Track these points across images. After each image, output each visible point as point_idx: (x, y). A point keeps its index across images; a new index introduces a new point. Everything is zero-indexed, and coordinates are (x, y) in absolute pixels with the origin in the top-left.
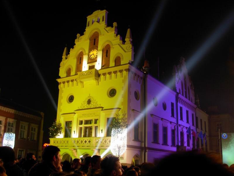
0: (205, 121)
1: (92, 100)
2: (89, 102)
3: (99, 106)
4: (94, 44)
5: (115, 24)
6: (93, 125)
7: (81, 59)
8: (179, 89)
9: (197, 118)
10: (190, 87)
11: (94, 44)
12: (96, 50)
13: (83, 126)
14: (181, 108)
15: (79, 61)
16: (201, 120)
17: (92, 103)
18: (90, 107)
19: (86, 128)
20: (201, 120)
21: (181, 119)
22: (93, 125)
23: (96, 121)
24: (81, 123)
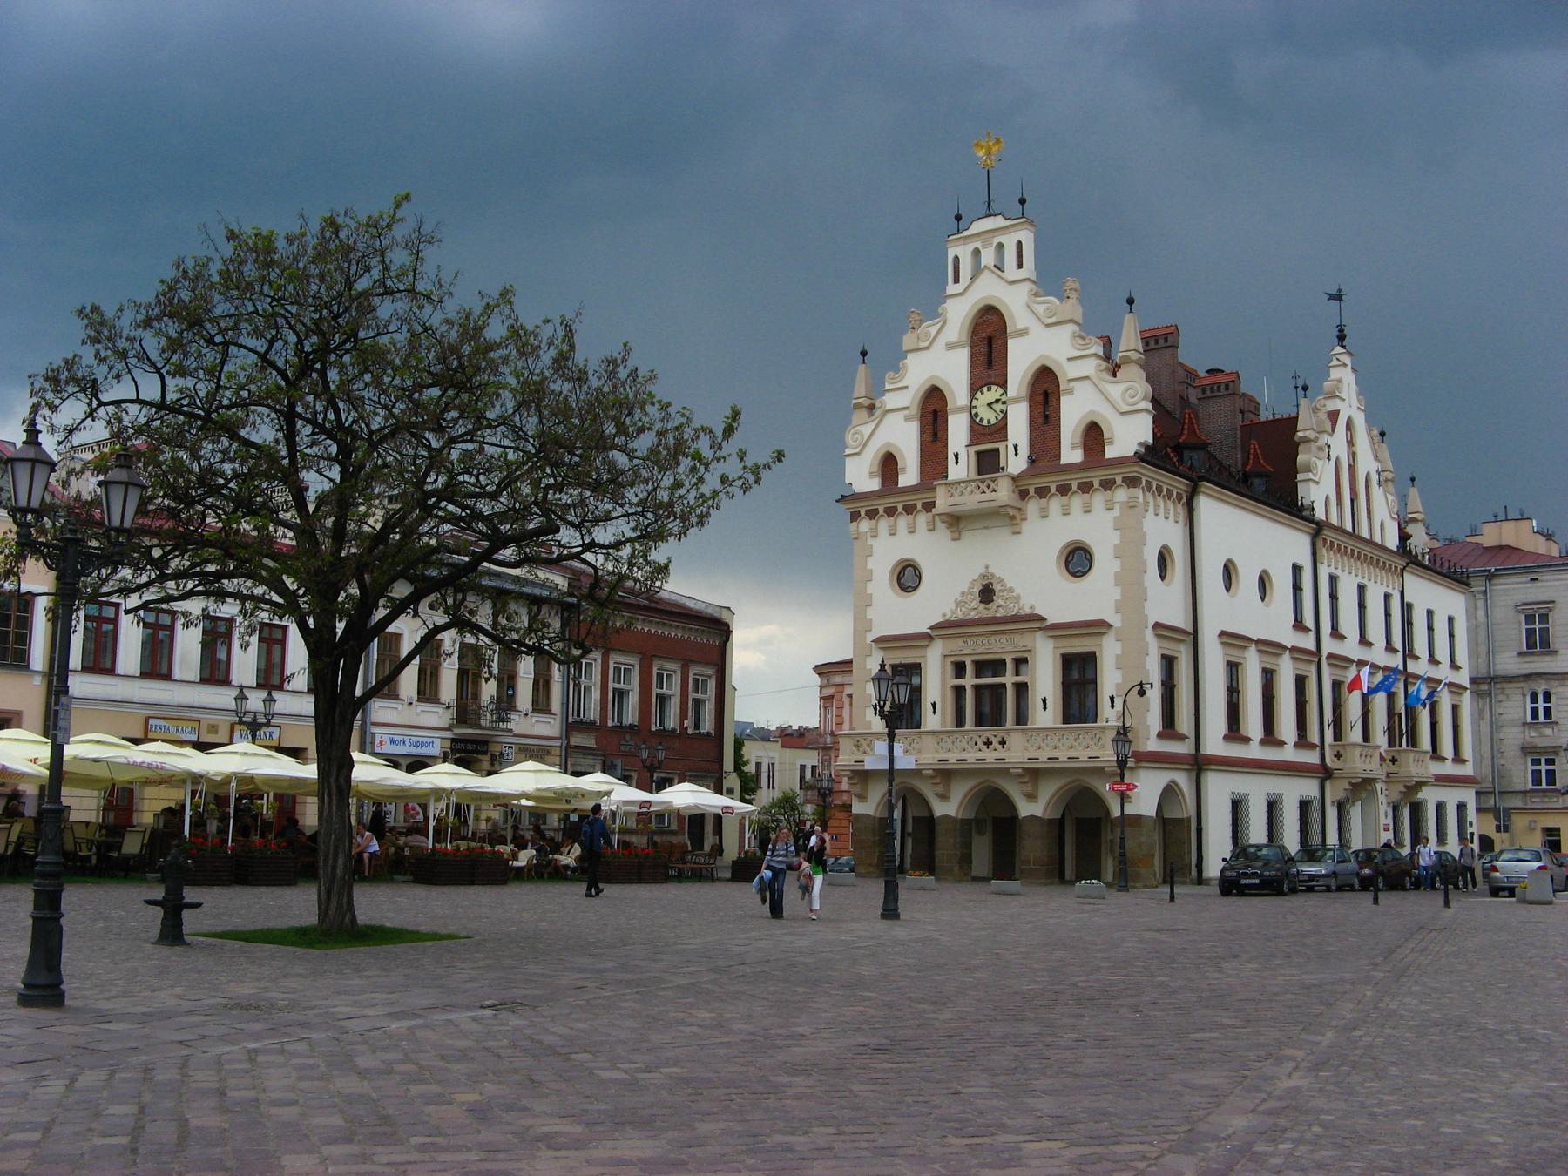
0: (1453, 614)
1: (997, 587)
2: (987, 594)
3: (1027, 610)
4: (990, 363)
5: (1071, 284)
6: (1009, 679)
7: (935, 420)
8: (1327, 498)
9: (1407, 609)
10: (1374, 478)
11: (990, 363)
12: (1000, 391)
13: (969, 681)
14: (1333, 579)
15: (930, 428)
16: (1430, 613)
17: (998, 601)
18: (990, 614)
19: (978, 689)
20: (1430, 613)
21: (1336, 634)
22: (1009, 679)
23: (1020, 662)
24: (959, 669)
